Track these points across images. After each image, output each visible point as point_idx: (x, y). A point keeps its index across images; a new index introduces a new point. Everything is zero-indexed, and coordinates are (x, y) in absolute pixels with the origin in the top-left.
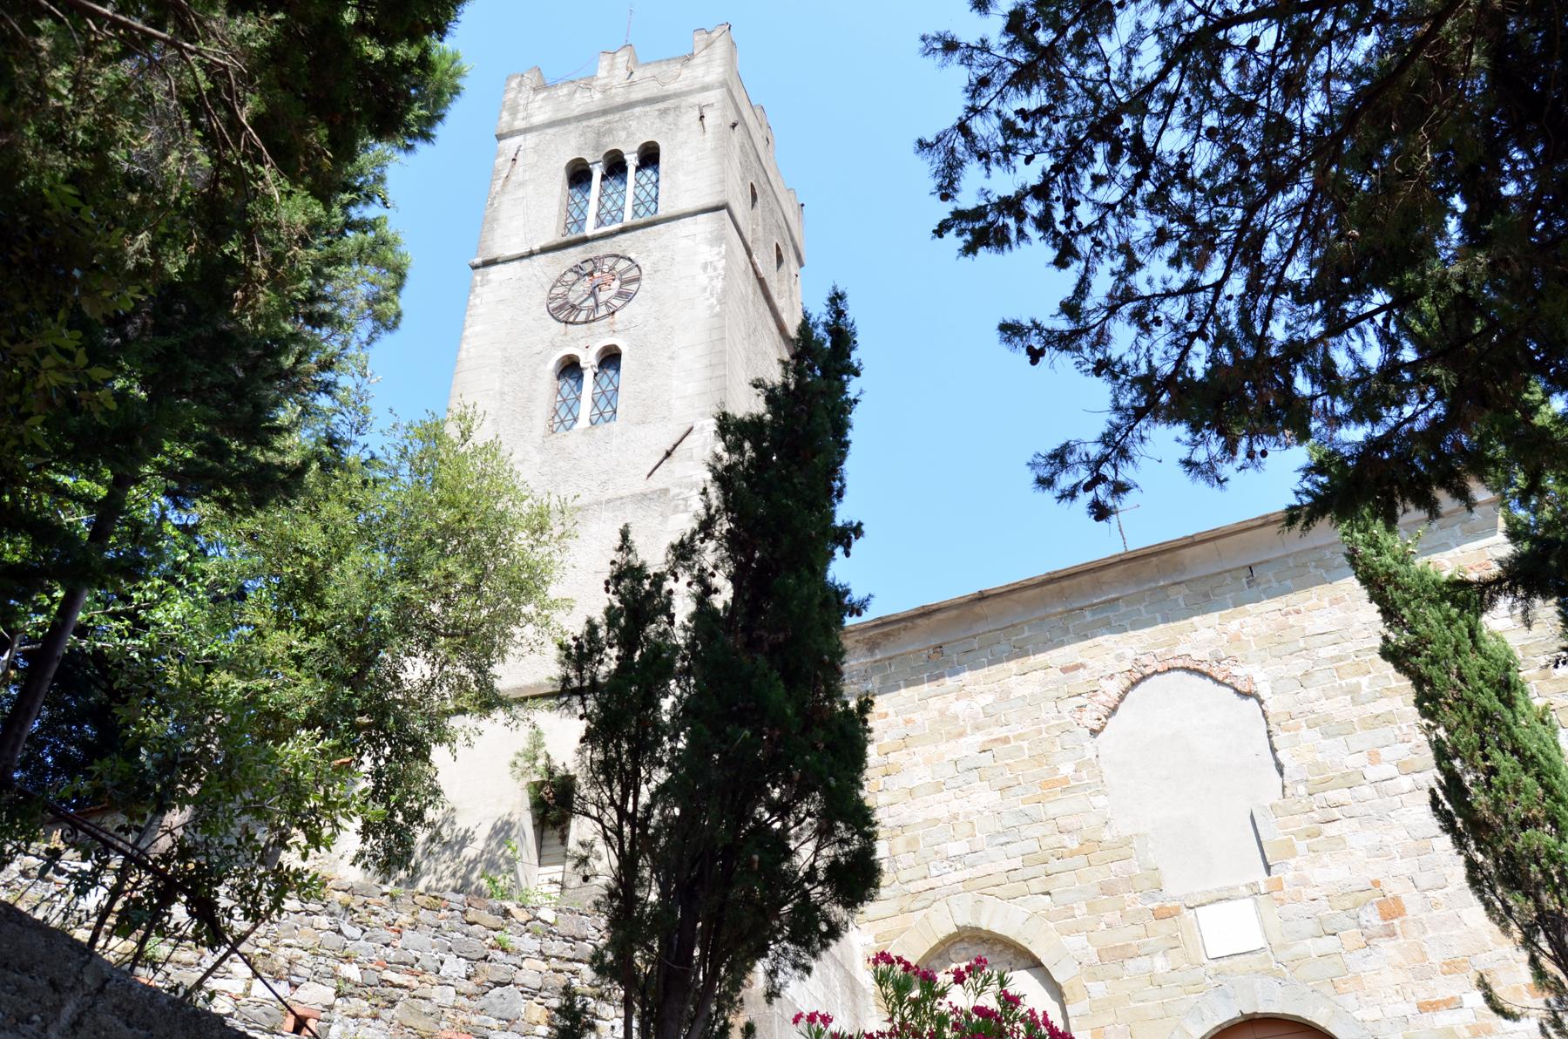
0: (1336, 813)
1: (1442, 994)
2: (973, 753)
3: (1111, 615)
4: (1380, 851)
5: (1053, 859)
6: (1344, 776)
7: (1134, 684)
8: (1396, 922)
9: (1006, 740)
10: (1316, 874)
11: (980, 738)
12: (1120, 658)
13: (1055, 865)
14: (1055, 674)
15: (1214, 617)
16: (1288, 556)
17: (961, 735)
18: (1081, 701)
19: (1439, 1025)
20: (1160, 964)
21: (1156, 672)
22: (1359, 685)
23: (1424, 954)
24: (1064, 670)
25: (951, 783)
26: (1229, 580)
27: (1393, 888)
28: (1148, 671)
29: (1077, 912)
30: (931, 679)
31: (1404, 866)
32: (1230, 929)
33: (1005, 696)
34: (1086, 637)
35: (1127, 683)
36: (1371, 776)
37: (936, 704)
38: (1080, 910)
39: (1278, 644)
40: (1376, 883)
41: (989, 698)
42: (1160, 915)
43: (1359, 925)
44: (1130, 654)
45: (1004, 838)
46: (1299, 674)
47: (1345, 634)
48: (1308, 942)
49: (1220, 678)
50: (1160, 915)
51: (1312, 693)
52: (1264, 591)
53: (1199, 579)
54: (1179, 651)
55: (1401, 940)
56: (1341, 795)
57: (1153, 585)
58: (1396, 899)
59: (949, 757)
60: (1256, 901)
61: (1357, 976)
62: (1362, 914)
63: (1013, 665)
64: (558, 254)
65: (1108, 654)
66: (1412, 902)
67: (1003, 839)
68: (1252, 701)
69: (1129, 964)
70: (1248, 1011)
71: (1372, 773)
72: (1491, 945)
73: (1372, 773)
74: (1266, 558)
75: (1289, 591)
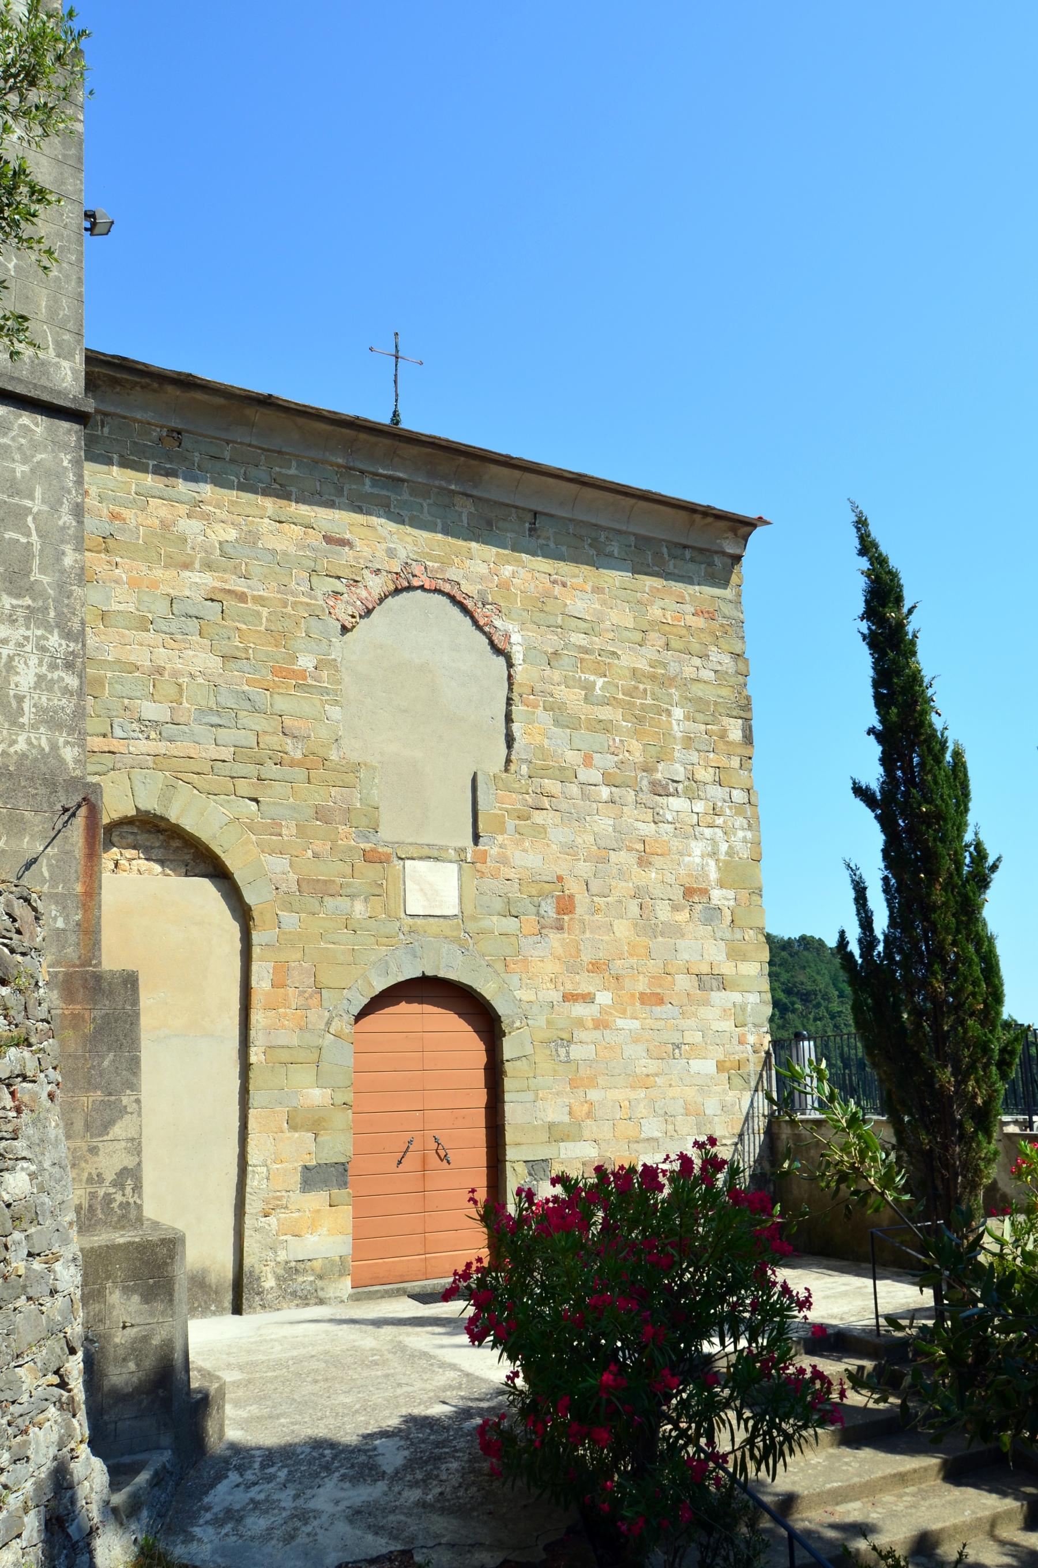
0: (546, 802)
1: (584, 988)
2: (198, 597)
3: (393, 496)
4: (570, 849)
5: (270, 763)
6: (562, 769)
7: (397, 591)
8: (566, 917)
9: (242, 597)
10: (518, 857)
11: (208, 580)
12: (391, 553)
13: (271, 770)
14: (315, 539)
15: (491, 552)
16: (570, 520)
17: (187, 566)
18: (339, 586)
19: (574, 1014)
20: (359, 909)
21: (422, 588)
22: (594, 683)
23: (579, 951)
24: (328, 539)
25: (162, 625)
26: (513, 517)
27: (573, 887)
28: (416, 582)
29: (284, 831)
30: (157, 471)
31: (584, 869)
32: (433, 888)
33: (251, 539)
34: (359, 510)
35: (392, 587)
36: (582, 777)
37: (159, 509)
38: (289, 831)
39: (541, 610)
40: (560, 879)
41: (232, 534)
42: (368, 857)
43: (538, 914)
44: (402, 554)
45: (218, 717)
46: (550, 650)
47: (597, 629)
48: (495, 918)
49: (481, 623)
50: (368, 857)
51: (557, 676)
52: (542, 547)
53: (487, 501)
54: (452, 573)
55: (566, 935)
56: (551, 785)
57: (443, 484)
58: (571, 897)
59: (165, 589)
60: (460, 868)
61: (525, 960)
62: (543, 904)
63: (269, 504)
64: (457, 1350)
65: (382, 542)
66: (582, 900)
67: (215, 720)
68: (501, 660)
69: (329, 901)
70: (429, 973)
71: (584, 775)
72: (626, 954)
73: (584, 775)
74: (553, 512)
75: (561, 558)
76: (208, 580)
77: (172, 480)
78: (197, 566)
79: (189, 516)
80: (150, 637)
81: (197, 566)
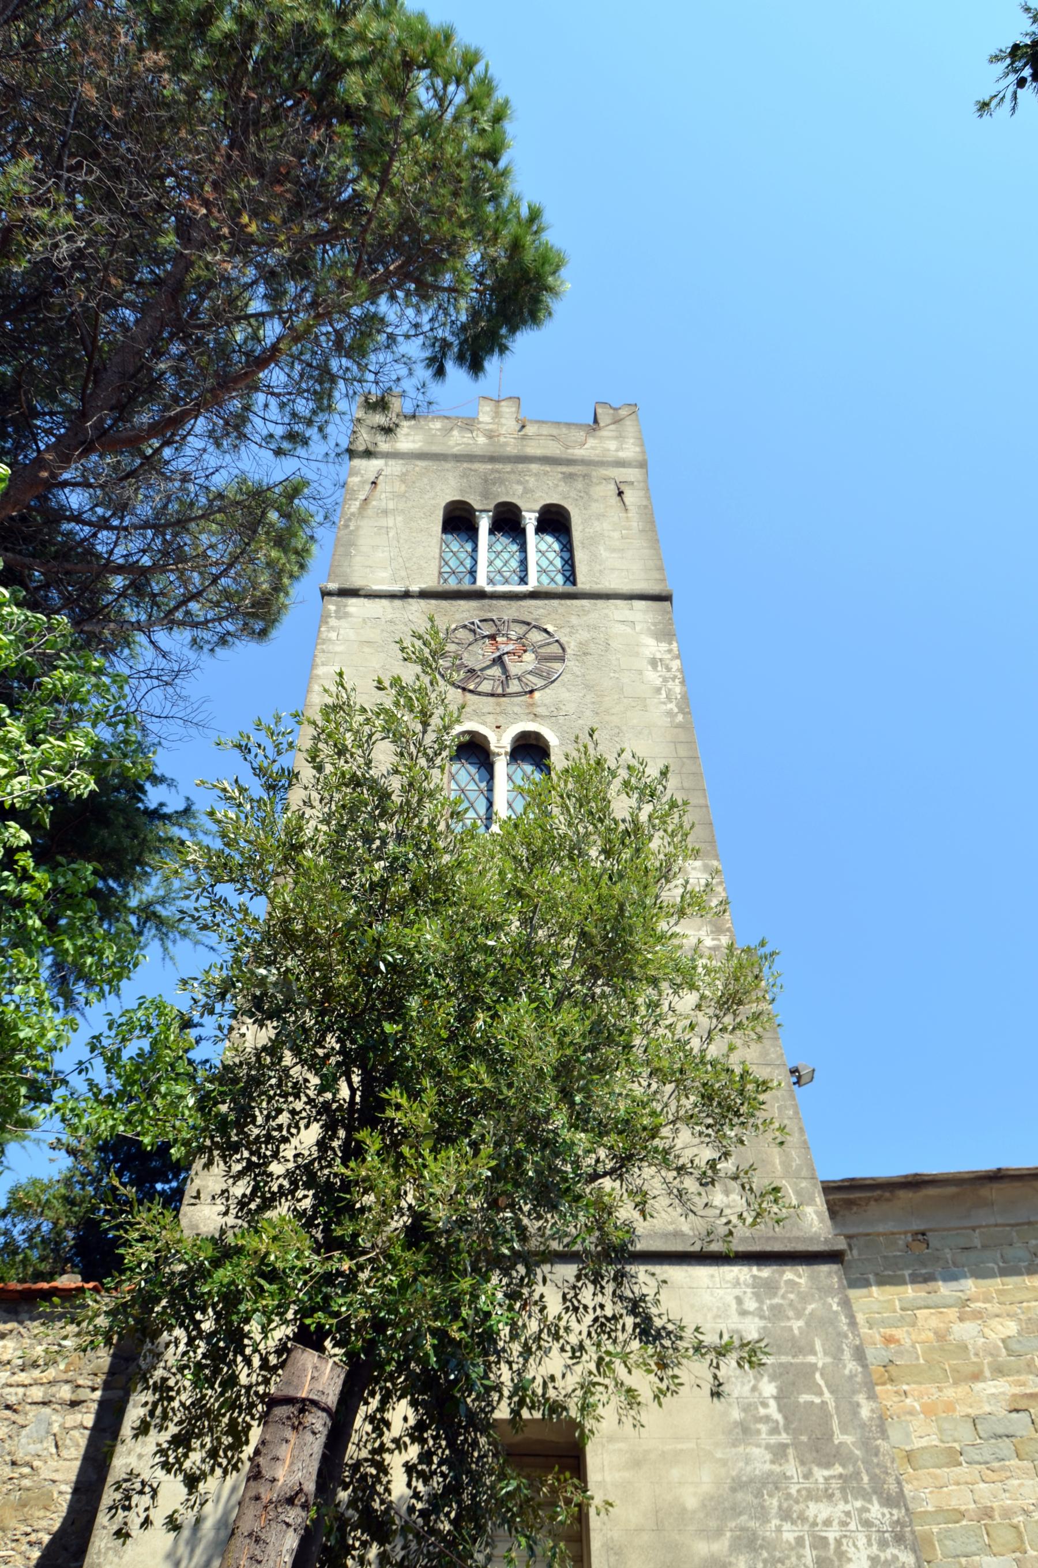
17: (977, 1377)
25: (973, 1454)
41: (1011, 1328)
59: (962, 1410)
76: (1000, 1388)
77: (931, 1285)
78: (987, 1373)
79: (961, 1319)
80: (963, 1471)
81: (987, 1373)
